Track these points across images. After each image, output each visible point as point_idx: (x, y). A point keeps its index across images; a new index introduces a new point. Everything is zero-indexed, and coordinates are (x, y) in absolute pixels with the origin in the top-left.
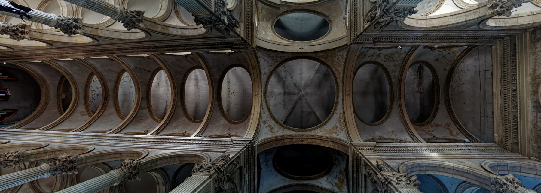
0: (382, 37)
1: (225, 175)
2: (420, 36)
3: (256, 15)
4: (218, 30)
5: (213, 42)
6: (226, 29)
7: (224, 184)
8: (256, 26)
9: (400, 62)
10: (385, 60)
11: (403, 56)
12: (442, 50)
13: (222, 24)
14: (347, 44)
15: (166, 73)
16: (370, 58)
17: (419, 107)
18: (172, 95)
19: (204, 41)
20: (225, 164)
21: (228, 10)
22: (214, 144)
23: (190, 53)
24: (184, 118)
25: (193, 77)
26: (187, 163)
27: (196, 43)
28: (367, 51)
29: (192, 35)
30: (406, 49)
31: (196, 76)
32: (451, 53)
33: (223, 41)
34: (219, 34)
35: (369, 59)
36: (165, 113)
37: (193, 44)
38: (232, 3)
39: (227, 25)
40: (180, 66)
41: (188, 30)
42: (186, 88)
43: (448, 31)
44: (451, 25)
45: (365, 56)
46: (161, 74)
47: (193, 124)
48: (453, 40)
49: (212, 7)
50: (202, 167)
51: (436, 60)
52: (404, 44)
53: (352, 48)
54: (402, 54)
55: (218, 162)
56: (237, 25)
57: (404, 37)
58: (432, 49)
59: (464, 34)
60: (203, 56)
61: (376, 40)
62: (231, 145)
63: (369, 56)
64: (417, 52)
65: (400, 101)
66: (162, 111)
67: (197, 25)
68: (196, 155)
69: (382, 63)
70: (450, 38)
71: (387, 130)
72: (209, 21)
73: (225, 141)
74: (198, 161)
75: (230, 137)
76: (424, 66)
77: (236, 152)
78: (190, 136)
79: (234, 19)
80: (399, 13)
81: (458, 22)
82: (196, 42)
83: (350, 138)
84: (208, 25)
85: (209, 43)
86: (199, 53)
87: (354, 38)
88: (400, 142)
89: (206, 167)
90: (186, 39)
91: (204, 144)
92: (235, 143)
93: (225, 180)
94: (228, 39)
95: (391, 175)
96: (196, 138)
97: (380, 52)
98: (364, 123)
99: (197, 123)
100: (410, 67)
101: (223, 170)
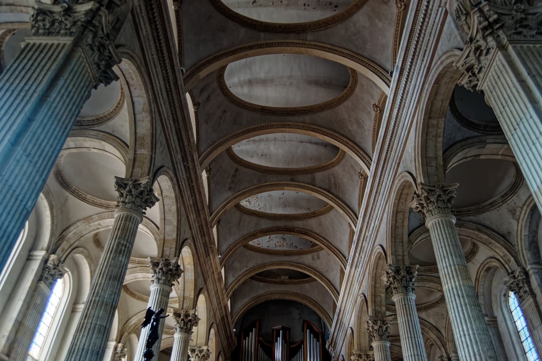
1: (511, 10)
5: (152, 43)
7: (534, 14)
18: (286, 132)
19: (155, 65)
20: (481, 11)
22: (417, 42)
23: (188, 95)
24: (342, 110)
25: (246, 90)
26: (448, 102)
27: (162, 82)
29: (143, 91)
31: (241, 84)
33: (146, 18)
36: (326, 145)
37: (166, 88)
40: (221, 118)
41: (135, 99)
42: (271, 105)
46: (242, 151)
47: (357, 90)
50: (470, 69)
55: (469, 28)
60: (191, 68)
66: (322, 150)
67: (117, 78)
68: (434, 83)
73: (417, 11)
74: (452, 77)
78: (386, 97)
82: (159, 83)
84: (110, 52)
85: (158, 55)
86: (185, 76)
89: (472, 60)
90: (157, 103)
91: (411, 66)
93: (523, 11)
96: (393, 84)
99: (355, 82)
101: (495, 16)
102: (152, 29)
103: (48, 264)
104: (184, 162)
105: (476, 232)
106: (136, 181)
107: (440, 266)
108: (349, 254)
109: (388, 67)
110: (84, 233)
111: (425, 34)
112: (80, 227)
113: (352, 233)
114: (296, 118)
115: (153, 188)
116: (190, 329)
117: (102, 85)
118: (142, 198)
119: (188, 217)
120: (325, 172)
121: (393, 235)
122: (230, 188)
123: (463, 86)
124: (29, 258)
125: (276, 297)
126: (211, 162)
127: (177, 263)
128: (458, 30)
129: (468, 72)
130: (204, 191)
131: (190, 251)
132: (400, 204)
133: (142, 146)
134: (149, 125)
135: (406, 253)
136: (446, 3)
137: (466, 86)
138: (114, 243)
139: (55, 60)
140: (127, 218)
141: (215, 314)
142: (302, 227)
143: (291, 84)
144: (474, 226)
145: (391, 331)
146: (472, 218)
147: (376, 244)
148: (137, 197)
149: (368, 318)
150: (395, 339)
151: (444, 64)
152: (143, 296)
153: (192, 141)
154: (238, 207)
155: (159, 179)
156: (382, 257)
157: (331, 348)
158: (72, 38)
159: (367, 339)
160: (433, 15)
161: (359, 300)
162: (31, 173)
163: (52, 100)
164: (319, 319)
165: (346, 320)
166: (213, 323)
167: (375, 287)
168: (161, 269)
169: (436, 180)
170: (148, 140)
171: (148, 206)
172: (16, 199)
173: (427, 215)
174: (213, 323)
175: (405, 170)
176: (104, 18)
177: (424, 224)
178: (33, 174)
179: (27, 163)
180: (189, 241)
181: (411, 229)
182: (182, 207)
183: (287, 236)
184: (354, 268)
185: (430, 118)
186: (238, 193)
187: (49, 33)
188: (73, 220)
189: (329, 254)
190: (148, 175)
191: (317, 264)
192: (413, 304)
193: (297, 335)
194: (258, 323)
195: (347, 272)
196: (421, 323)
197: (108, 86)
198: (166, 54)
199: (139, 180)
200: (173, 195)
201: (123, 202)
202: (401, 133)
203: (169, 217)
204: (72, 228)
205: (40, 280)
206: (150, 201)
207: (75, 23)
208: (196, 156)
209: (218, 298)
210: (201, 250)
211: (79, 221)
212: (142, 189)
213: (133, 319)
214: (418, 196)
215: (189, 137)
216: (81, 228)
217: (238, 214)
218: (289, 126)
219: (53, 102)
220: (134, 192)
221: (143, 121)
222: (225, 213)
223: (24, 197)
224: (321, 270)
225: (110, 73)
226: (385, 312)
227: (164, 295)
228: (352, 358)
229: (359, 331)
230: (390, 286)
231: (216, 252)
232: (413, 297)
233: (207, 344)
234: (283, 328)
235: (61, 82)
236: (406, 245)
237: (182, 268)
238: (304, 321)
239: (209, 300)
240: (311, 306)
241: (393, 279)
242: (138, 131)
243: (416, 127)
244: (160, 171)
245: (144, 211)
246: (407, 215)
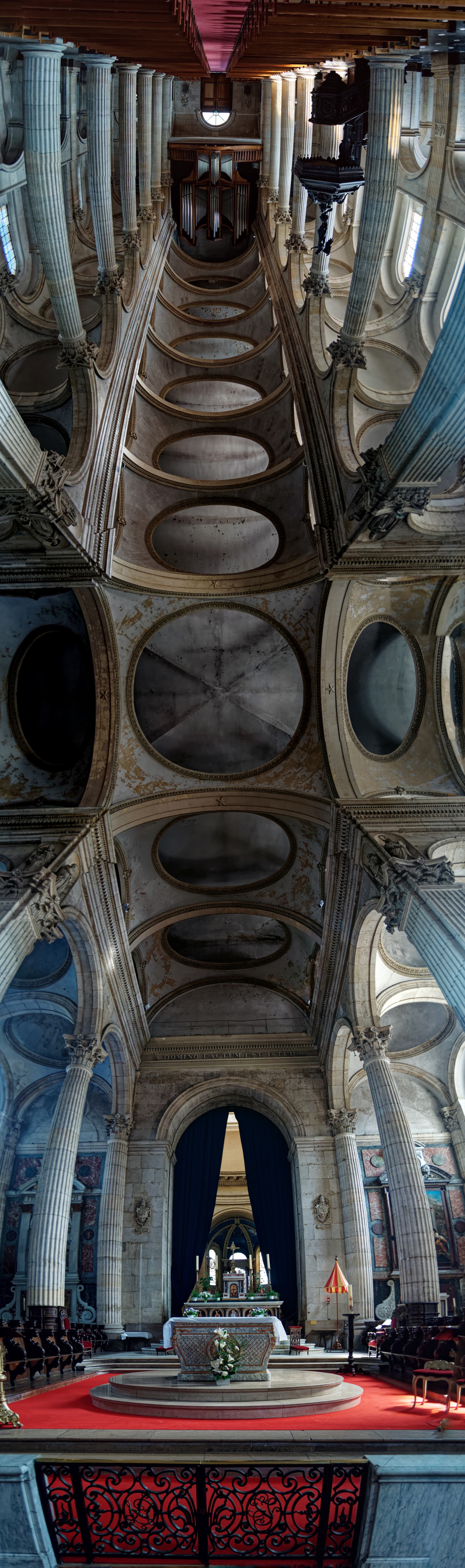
0: (348, 871)
2: (339, 937)
9: (291, 904)
10: (297, 877)
11: (304, 911)
12: (309, 971)
16: (303, 846)
17: (200, 938)
28: (319, 841)
30: (316, 915)
32: (301, 984)
35: (300, 845)
43: (343, 978)
44: (353, 983)
45: (309, 836)
48: (324, 987)
51: (290, 964)
52: (328, 911)
54: (308, 908)
57: (343, 910)
58: (313, 957)
59: (332, 1000)
61: (342, 859)
63: (306, 845)
64: (309, 932)
65: (209, 906)
69: (292, 872)
70: (328, 982)
71: (145, 884)
76: (280, 946)
80: (395, 900)
81: (356, 992)
88: (125, 908)
95: (52, 894)
97: (315, 866)
98: (157, 839)
100: (280, 922)
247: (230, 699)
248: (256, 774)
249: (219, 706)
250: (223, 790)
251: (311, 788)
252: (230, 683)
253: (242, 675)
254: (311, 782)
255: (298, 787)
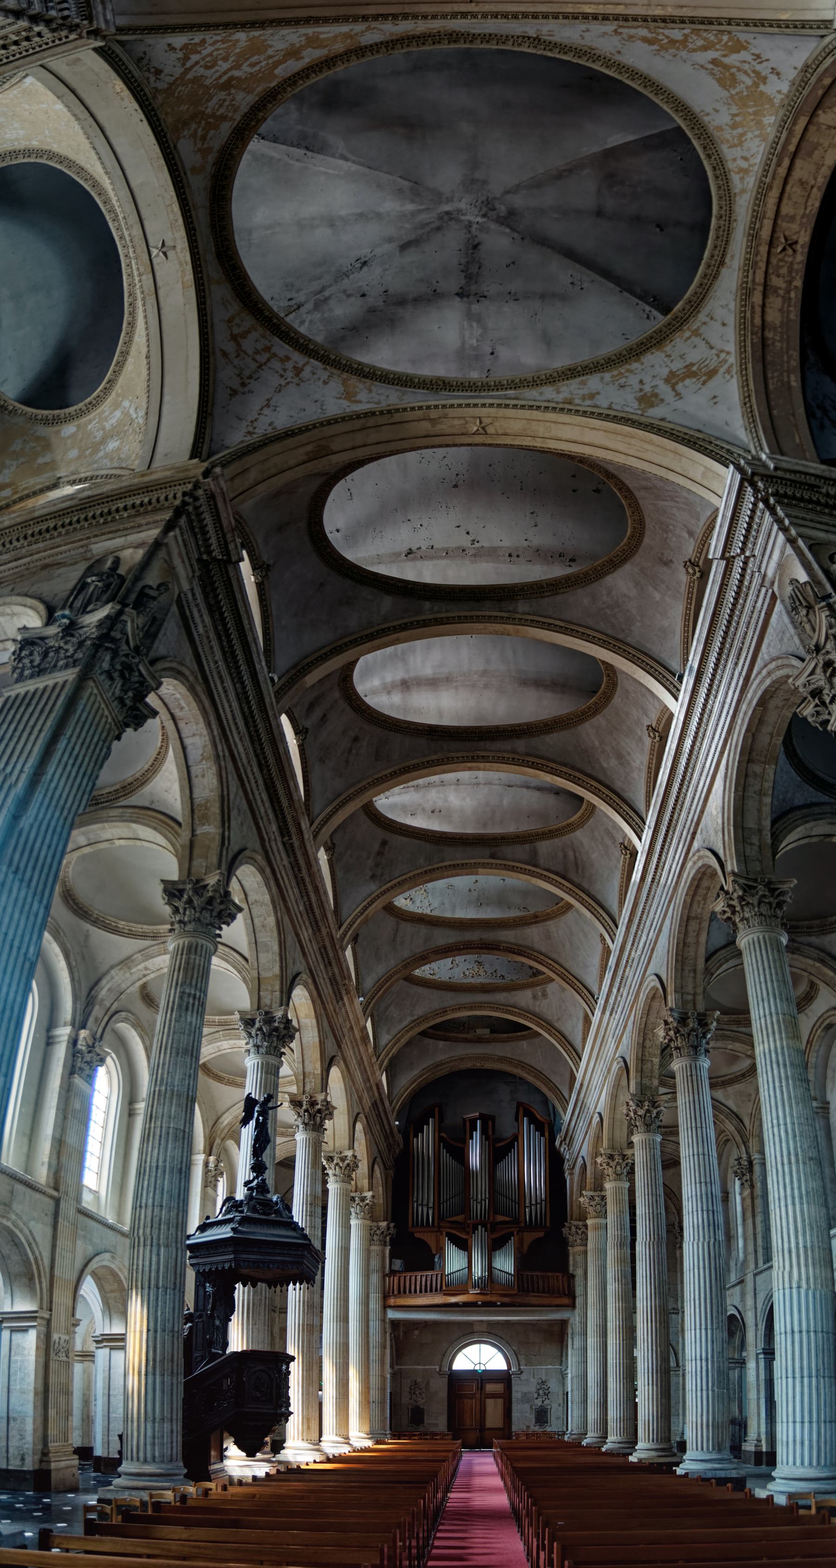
3: (30, 503)
4: (151, 633)
5: (215, 643)
6: (140, 603)
8: (89, 489)
13: (119, 626)
14: (95, 50)
15: (388, 789)
18: (479, 769)
19: (221, 677)
21: (50, 620)
22: (726, 633)
23: (284, 719)
24: (588, 731)
25: (396, 698)
26: (781, 738)
27: (235, 704)
31: (388, 689)
33: (202, 606)
34: (171, 629)
36: (558, 792)
37: (243, 713)
38: (13, 615)
39: (118, 607)
40: (350, 750)
41: (188, 741)
42: (446, 722)
46: (393, 807)
47: (617, 700)
49: (60, 681)
53: (122, 21)
56: (109, 563)
60: (288, 671)
62: (745, 563)
66: (551, 800)
67: (154, 713)
68: (757, 705)
72: (122, 676)
74: (788, 700)
75: (709, 563)
77: (789, 550)
79: (82, 586)
82: (230, 707)
83: (804, 24)
84: (141, 675)
85: (225, 660)
86: (277, 687)
87: (50, 35)
90: (227, 740)
91: (715, 670)
92: (743, 550)
94: (186, 586)
96: (684, 695)
102: (214, 621)
103: (79, 1047)
104: (283, 836)
105: (818, 964)
106: (198, 881)
107: (754, 1014)
108: (600, 989)
109: (675, 665)
110: (124, 986)
111: (738, 623)
112: (116, 978)
113: (607, 952)
114: (499, 745)
115: (230, 889)
116: (321, 1125)
117: (129, 731)
118: (212, 911)
119: (297, 935)
120: (556, 840)
121: (680, 958)
122: (373, 877)
123: (805, 719)
124: (49, 1042)
125: (469, 1065)
126: (335, 831)
127: (285, 1015)
128: (796, 628)
129: (814, 697)
130: (324, 885)
131: (307, 994)
132: (695, 906)
133: (205, 819)
134: (215, 782)
135: (700, 990)
136: (773, 583)
137: (810, 719)
138: (175, 995)
139: (51, 711)
140: (190, 947)
141: (360, 1098)
142: (513, 940)
143: (486, 686)
144: (815, 953)
145: (665, 1118)
146: (814, 940)
147: (648, 973)
148: (203, 909)
149: (628, 1097)
150: (671, 1131)
151: (774, 677)
152: (236, 1078)
153: (295, 798)
154: (390, 909)
155: (239, 872)
156: (658, 995)
157: (564, 1146)
158: (77, 670)
159: (625, 1130)
160: (751, 597)
161: (615, 1067)
162: (25, 899)
163: (49, 777)
164: (545, 1101)
165: (591, 1102)
166: (358, 1114)
167: (644, 1047)
168: (260, 1029)
169: (758, 869)
170: (215, 809)
171: (224, 923)
172: (11, 947)
173: (740, 925)
174: (358, 1114)
175: (705, 845)
176: (129, 624)
177: (734, 942)
178: (29, 900)
179: (17, 883)
180: (304, 976)
181: (711, 949)
182: (286, 919)
183: (486, 958)
184: (608, 1013)
185: (749, 761)
186: (390, 884)
187: (40, 672)
188: (103, 968)
189: (563, 990)
190: (219, 867)
191: (542, 1007)
192: (705, 1075)
193: (506, 1126)
194: (437, 1109)
195: (595, 1020)
196: (714, 1107)
197: (140, 729)
198: (240, 656)
199: (203, 880)
200: (267, 898)
201: (180, 922)
202: (699, 780)
203: (263, 937)
204: (104, 982)
205: (72, 1073)
206: (227, 915)
207: (81, 644)
208: (305, 824)
209: (364, 1071)
210: (327, 990)
211: (112, 967)
212: (210, 894)
213: (225, 1116)
214: (727, 893)
215: (290, 793)
216: (117, 979)
217: (391, 921)
218: (485, 759)
219: (51, 781)
220: (196, 901)
221: (203, 776)
222: (366, 922)
223: (21, 942)
224: (550, 1018)
225: (142, 708)
226: (657, 1088)
227: (270, 1072)
228: (599, 1160)
229: (613, 1119)
230: (668, 1045)
231: (353, 992)
232: (705, 1063)
233: (351, 1147)
234: (482, 1117)
235: (62, 744)
236: (700, 976)
237: (295, 1023)
238: (519, 1104)
239: (348, 1075)
240: (530, 1078)
241: (675, 1033)
242: (195, 796)
243: (726, 774)
244: (240, 858)
245: (218, 932)
246: (705, 924)
247: (438, 197)
248: (360, 51)
249: (471, 184)
250: (464, 15)
251: (185, 47)
252: (439, 229)
253: (404, 247)
254: (186, 58)
255: (223, 42)
